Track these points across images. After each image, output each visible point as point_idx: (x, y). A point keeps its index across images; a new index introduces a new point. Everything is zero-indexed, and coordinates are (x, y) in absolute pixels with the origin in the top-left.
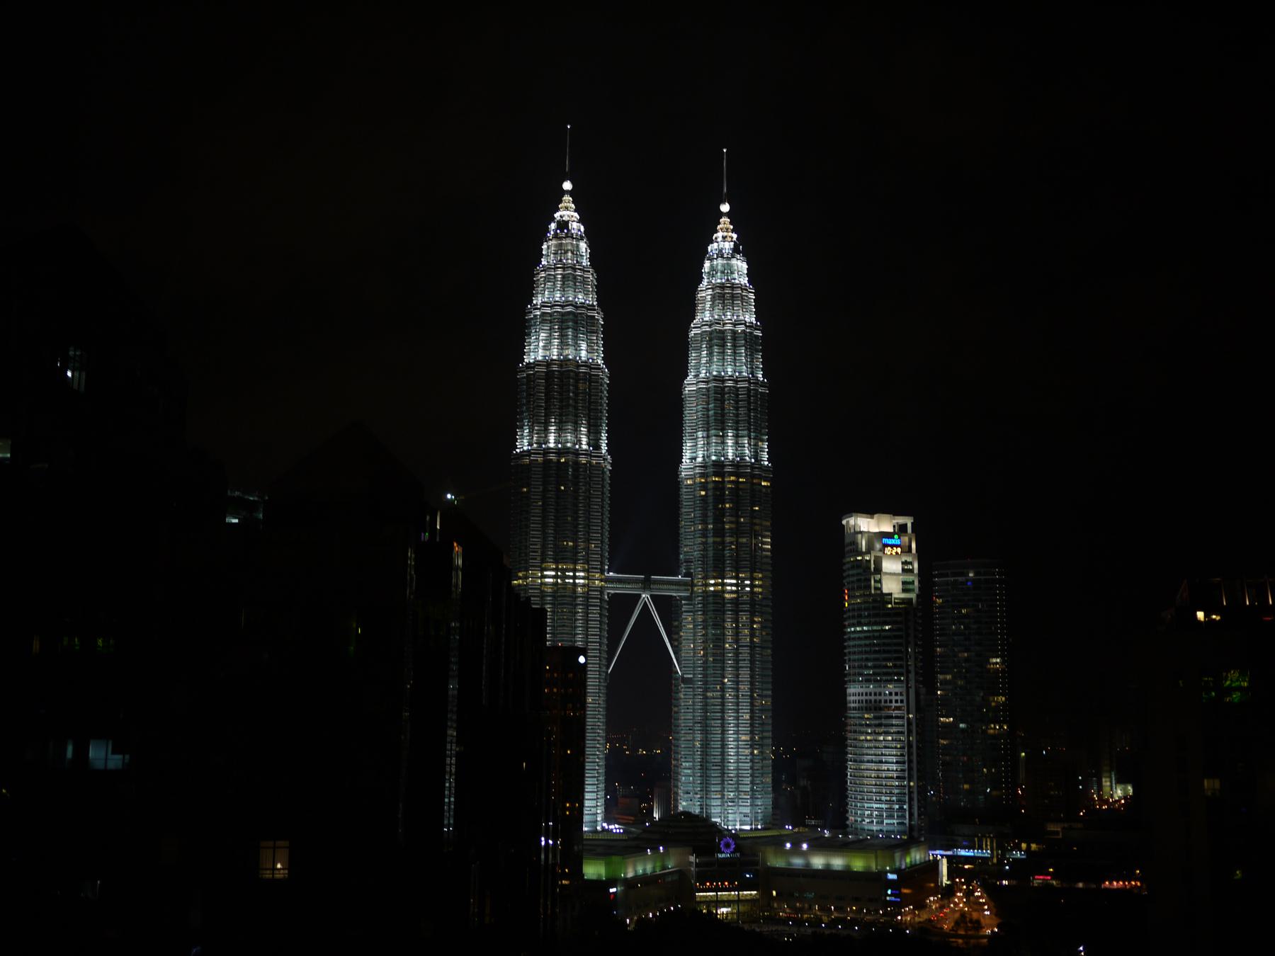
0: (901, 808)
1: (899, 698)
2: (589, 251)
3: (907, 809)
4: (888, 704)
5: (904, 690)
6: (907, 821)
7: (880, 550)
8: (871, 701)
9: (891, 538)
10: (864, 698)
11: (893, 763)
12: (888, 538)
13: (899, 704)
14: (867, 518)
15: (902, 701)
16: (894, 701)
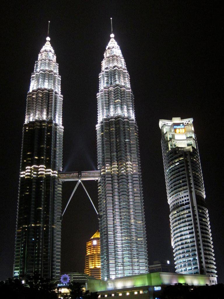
0: (195, 259)
1: (186, 198)
2: (55, 57)
3: (198, 259)
4: (182, 203)
5: (188, 194)
6: (198, 266)
7: (174, 132)
8: (175, 204)
9: (179, 126)
10: (173, 204)
11: (187, 234)
12: (177, 126)
13: (187, 201)
14: (168, 121)
15: (188, 200)
16: (184, 201)
